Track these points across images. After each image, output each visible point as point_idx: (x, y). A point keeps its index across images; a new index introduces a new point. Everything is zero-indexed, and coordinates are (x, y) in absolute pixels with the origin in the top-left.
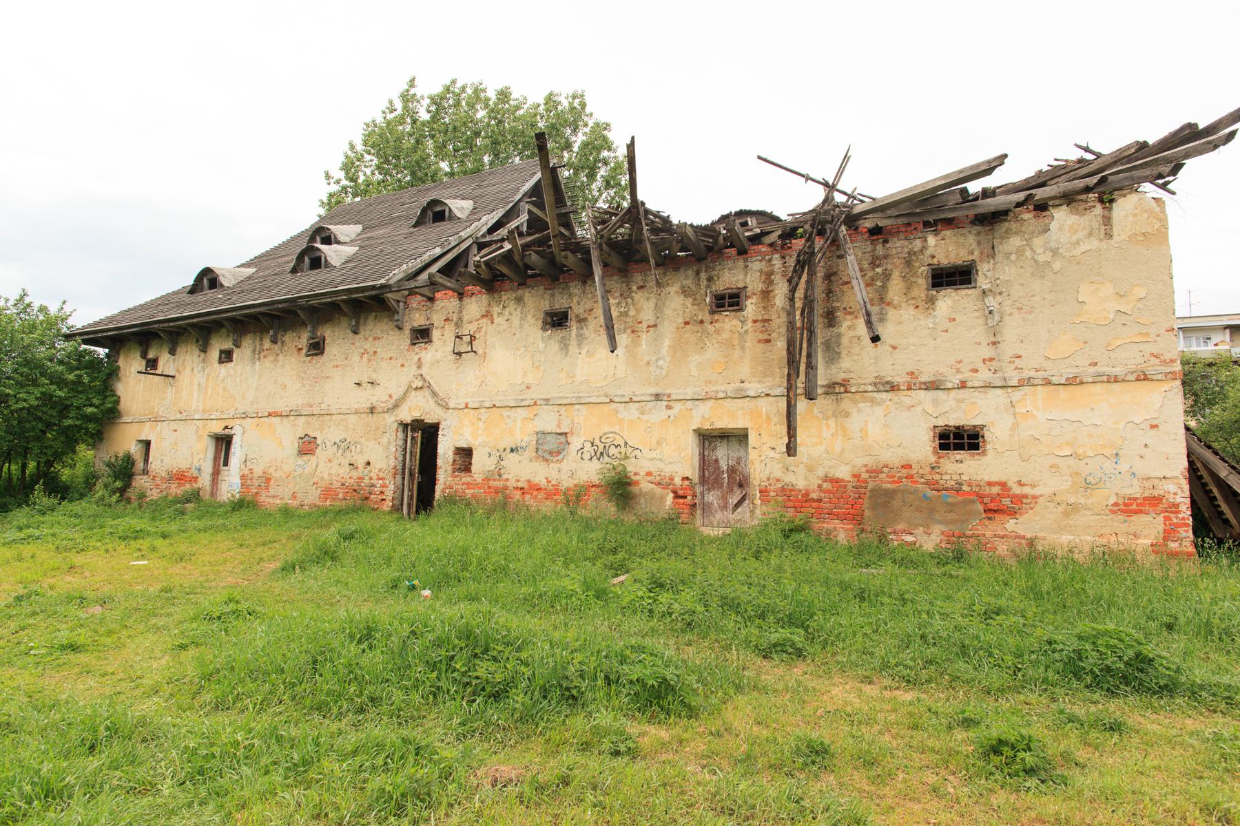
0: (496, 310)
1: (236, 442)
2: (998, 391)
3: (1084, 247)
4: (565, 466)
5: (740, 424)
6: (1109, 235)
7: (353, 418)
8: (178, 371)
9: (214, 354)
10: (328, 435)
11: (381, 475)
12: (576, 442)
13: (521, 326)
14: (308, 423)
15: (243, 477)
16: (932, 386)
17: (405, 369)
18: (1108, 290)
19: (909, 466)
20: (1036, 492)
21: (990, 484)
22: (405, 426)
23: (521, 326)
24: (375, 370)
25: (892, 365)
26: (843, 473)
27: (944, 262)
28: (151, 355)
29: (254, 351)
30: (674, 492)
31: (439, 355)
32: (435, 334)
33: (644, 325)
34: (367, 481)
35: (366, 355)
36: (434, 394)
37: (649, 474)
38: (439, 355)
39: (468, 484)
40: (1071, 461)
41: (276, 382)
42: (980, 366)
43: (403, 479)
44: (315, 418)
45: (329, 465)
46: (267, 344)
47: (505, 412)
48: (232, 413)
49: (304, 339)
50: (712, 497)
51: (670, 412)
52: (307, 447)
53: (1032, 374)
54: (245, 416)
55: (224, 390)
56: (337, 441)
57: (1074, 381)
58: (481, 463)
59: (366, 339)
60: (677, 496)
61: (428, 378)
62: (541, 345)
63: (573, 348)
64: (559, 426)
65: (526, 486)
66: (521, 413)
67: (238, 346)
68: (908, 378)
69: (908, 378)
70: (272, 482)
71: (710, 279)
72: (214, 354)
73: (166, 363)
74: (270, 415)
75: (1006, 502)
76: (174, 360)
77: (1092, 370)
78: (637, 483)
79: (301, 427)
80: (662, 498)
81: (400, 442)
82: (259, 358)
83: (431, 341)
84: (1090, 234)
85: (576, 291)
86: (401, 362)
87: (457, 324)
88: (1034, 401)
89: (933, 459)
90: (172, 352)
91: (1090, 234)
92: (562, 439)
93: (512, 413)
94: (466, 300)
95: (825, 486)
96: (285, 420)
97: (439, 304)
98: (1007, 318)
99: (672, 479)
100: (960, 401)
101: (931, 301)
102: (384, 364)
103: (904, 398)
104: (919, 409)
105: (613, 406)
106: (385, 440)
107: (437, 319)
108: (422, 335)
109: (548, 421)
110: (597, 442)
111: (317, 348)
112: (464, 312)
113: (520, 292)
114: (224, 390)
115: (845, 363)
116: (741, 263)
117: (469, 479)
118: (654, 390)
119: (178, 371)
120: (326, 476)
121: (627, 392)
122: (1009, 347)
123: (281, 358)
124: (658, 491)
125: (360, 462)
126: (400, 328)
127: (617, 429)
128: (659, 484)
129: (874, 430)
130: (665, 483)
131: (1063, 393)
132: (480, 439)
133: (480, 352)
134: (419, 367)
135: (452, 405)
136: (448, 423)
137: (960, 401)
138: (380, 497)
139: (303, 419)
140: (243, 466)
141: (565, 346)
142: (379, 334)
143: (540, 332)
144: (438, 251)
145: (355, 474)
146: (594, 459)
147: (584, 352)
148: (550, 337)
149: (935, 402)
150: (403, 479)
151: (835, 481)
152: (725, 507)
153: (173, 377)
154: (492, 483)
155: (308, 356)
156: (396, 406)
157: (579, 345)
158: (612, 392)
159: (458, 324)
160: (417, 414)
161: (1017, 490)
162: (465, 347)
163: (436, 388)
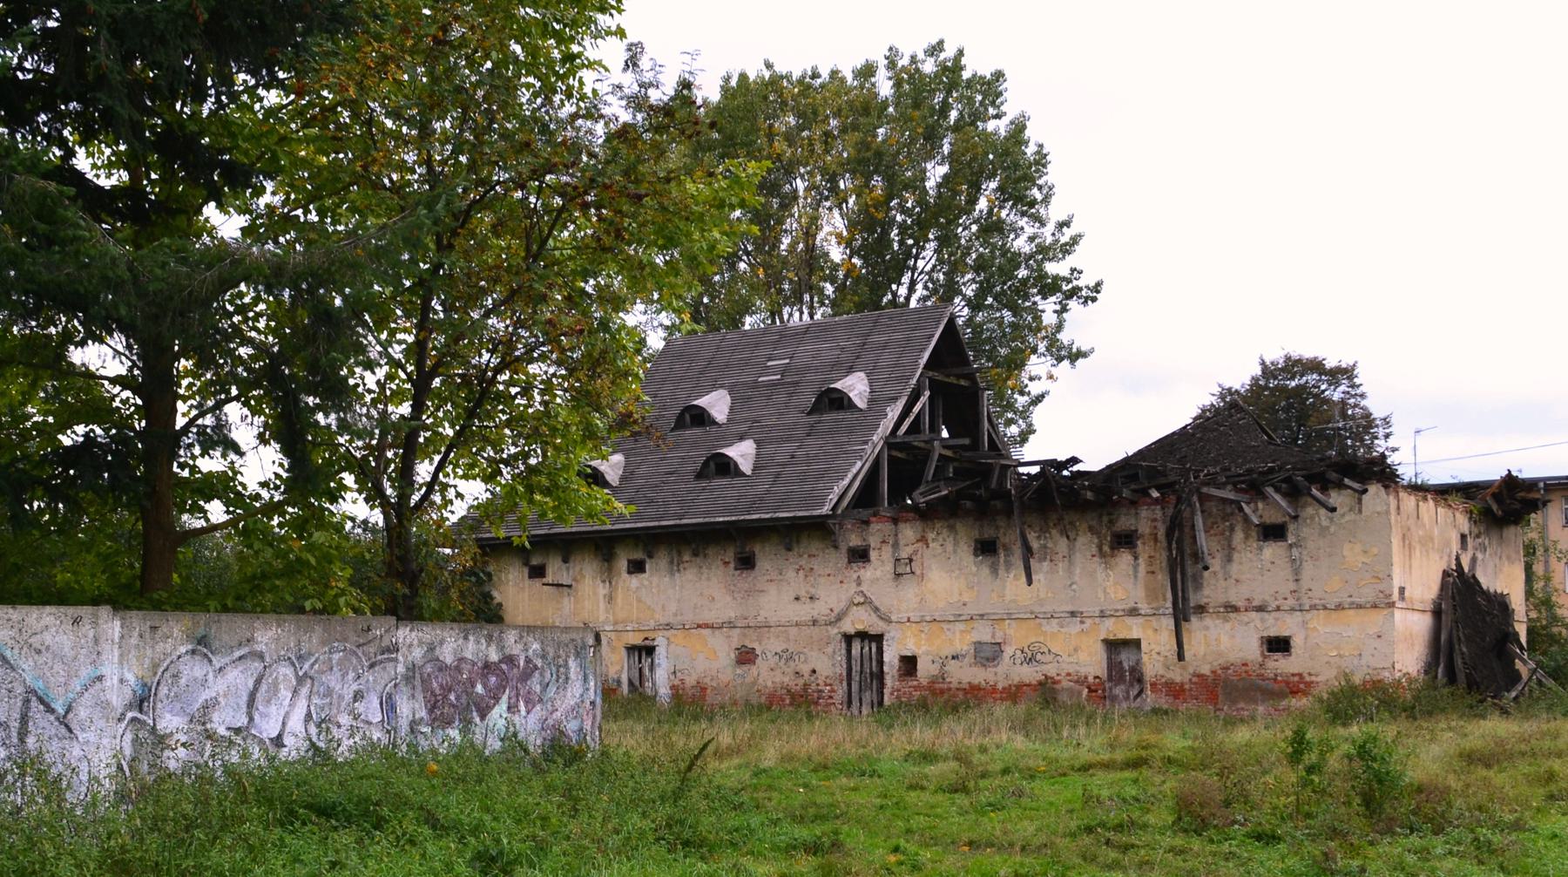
0: (931, 536)
1: (661, 652)
2: (1298, 613)
3: (1347, 518)
4: (1000, 669)
5: (1135, 636)
6: (1360, 511)
7: (793, 631)
8: (575, 580)
9: (622, 564)
10: (767, 647)
11: (828, 681)
12: (1009, 651)
13: (955, 552)
14: (745, 635)
15: (673, 687)
16: (1261, 609)
17: (845, 586)
18: (1358, 548)
19: (1245, 665)
20: (1318, 679)
21: (1293, 675)
22: (848, 639)
23: (955, 551)
24: (813, 586)
25: (1236, 596)
26: (1205, 670)
27: (1268, 521)
28: (535, 561)
29: (672, 562)
30: (1089, 687)
31: (878, 573)
32: (873, 555)
33: (1060, 555)
34: (813, 687)
35: (801, 572)
36: (876, 609)
37: (1069, 674)
38: (878, 573)
39: (915, 687)
40: (1337, 659)
41: (701, 594)
42: (1289, 596)
43: (849, 685)
44: (751, 630)
45: (772, 673)
46: (686, 557)
47: (945, 626)
48: (652, 624)
49: (730, 555)
50: (1119, 691)
51: (1083, 626)
52: (746, 657)
53: (1317, 602)
54: (669, 627)
55: (639, 601)
56: (779, 651)
57: (1339, 607)
58: (925, 669)
59: (801, 556)
60: (1091, 691)
61: (868, 594)
62: (974, 569)
63: (1001, 572)
64: (993, 636)
65: (967, 687)
66: (960, 626)
67: (651, 557)
68: (1246, 603)
69: (1246, 603)
70: (709, 691)
71: (1111, 522)
72: (622, 564)
73: (556, 570)
74: (699, 626)
75: (1302, 686)
76: (568, 569)
77: (1349, 600)
78: (1059, 682)
79: (736, 638)
80: (1080, 693)
81: (844, 652)
82: (679, 570)
83: (869, 561)
84: (1351, 510)
85: (1002, 524)
86: (840, 578)
87: (893, 546)
88: (1317, 621)
89: (1260, 659)
90: (565, 561)
91: (1351, 510)
92: (997, 648)
93: (951, 626)
94: (901, 526)
95: (1195, 679)
96: (717, 632)
97: (875, 527)
98: (1304, 564)
99: (1086, 678)
100: (1277, 619)
101: (1261, 549)
102: (822, 580)
103: (1245, 617)
104: (1252, 625)
105: (1038, 621)
106: (830, 650)
107: (873, 541)
108: (860, 555)
109: (983, 633)
110: (1026, 650)
111: (746, 563)
112: (900, 535)
113: (952, 521)
114: (639, 601)
115: (1206, 591)
116: (1133, 511)
117: (915, 683)
118: (1070, 608)
119: (575, 580)
120: (769, 684)
121: (1048, 608)
122: (1306, 583)
123: (704, 570)
124: (1077, 687)
125: (805, 669)
126: (836, 547)
127: (1041, 639)
128: (1077, 682)
129: (1224, 639)
130: (1081, 681)
131: (1334, 615)
132: (924, 648)
133: (918, 572)
134: (859, 584)
135: (894, 618)
136: (892, 634)
137: (1277, 619)
138: (830, 701)
139: (737, 631)
140: (672, 677)
141: (994, 571)
142: (814, 551)
143: (972, 557)
144: (859, 464)
145: (801, 682)
146: (1025, 665)
147: (1012, 576)
148: (981, 562)
149: (1262, 620)
150: (849, 685)
151: (1200, 676)
152: (1127, 698)
153: (570, 586)
154: (937, 686)
155: (736, 569)
156: (839, 618)
157: (1008, 570)
158: (1037, 609)
159: (896, 546)
160: (860, 627)
161: (1308, 679)
162: (903, 570)
163: (877, 603)
